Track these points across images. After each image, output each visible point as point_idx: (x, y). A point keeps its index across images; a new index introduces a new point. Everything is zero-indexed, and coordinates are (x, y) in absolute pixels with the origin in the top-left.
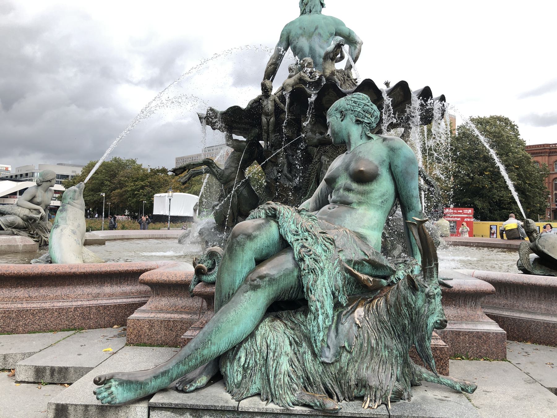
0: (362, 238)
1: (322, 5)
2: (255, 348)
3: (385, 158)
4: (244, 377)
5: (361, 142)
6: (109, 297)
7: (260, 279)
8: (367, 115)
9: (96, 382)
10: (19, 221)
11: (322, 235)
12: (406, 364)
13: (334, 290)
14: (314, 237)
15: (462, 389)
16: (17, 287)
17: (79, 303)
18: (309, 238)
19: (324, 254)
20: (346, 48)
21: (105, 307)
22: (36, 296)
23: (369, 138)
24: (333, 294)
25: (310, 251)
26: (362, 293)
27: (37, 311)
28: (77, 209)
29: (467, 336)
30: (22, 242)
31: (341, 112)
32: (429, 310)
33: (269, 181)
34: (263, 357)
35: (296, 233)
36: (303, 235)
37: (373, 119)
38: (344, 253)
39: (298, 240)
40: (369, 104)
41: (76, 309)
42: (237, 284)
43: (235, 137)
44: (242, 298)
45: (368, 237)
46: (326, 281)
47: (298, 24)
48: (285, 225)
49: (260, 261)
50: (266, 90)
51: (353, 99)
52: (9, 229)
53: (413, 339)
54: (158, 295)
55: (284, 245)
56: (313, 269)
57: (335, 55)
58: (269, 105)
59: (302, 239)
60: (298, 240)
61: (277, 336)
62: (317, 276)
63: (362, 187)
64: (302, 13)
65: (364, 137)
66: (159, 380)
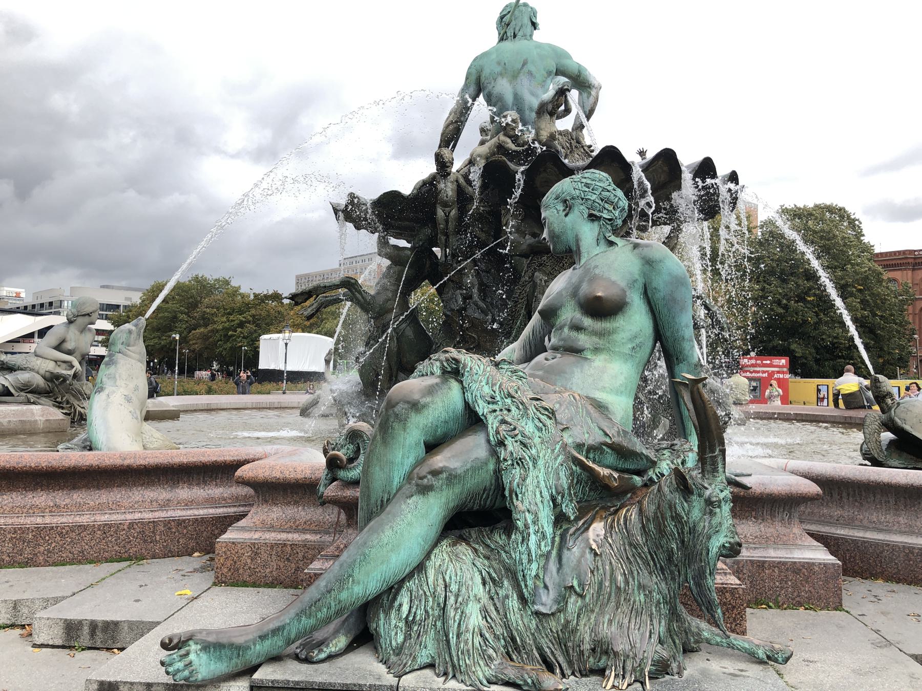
0: (601, 407)
1: (534, 25)
2: (426, 588)
3: (637, 277)
4: (407, 637)
5: (597, 250)
6: (186, 505)
7: (433, 476)
8: (606, 206)
9: (165, 646)
10: (39, 381)
11: (535, 402)
12: (674, 615)
13: (554, 493)
14: (521, 407)
15: (769, 657)
16: (34, 489)
17: (137, 516)
18: (513, 408)
19: (537, 433)
20: (574, 95)
21: (180, 523)
22: (67, 505)
23: (611, 244)
24: (553, 499)
25: (515, 429)
26: (601, 498)
27: (67, 529)
28: (133, 361)
29: (776, 570)
31: (565, 201)
32: (711, 526)
33: (448, 313)
34: (439, 604)
35: (492, 400)
36: (504, 403)
37: (617, 213)
38: (570, 433)
39: (495, 411)
40: (609, 188)
41: (132, 525)
42: (395, 483)
43: (393, 241)
44: (403, 506)
45: (610, 406)
46: (541, 478)
47: (494, 56)
48: (474, 386)
49: (432, 446)
50: (443, 165)
51: (584, 180)
52: (22, 393)
53: (686, 574)
54: (266, 501)
55: (472, 420)
56: (520, 459)
57: (555, 107)
58: (448, 189)
59: (501, 410)
60: (495, 411)
61: (461, 569)
62: (526, 470)
63: (599, 324)
64: (502, 39)
65: (602, 242)
66: (267, 643)
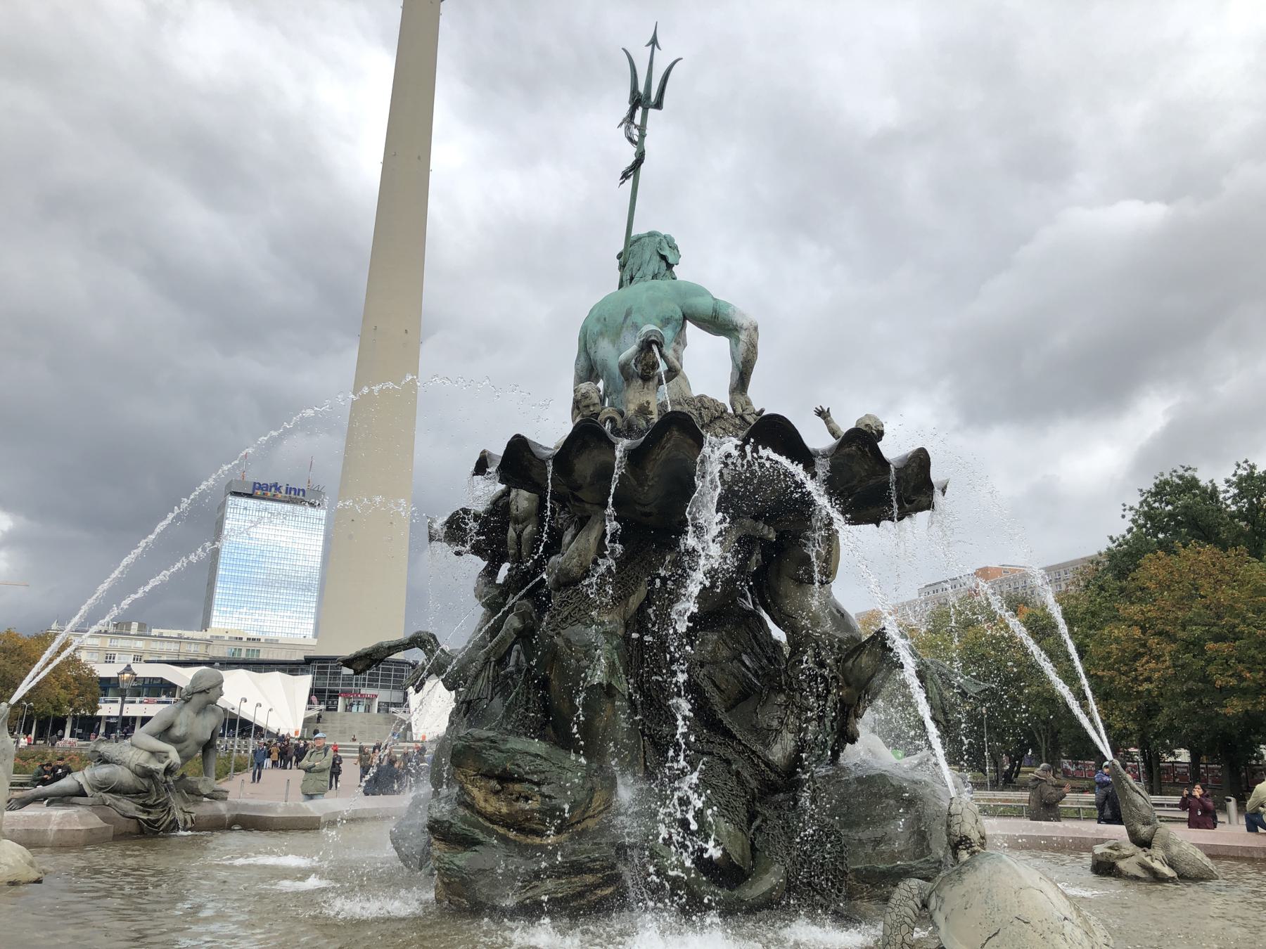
10: (123, 776)
30: (59, 824)
